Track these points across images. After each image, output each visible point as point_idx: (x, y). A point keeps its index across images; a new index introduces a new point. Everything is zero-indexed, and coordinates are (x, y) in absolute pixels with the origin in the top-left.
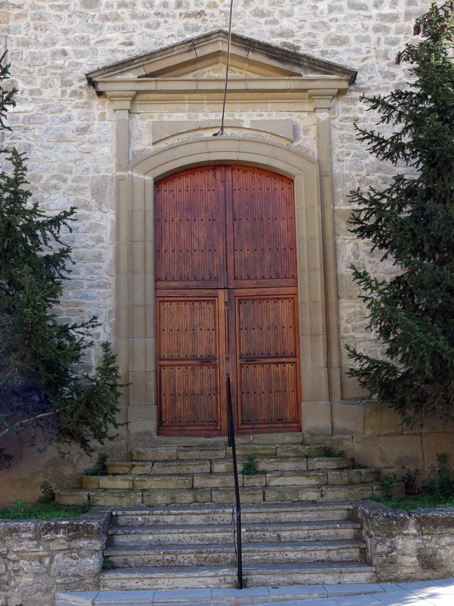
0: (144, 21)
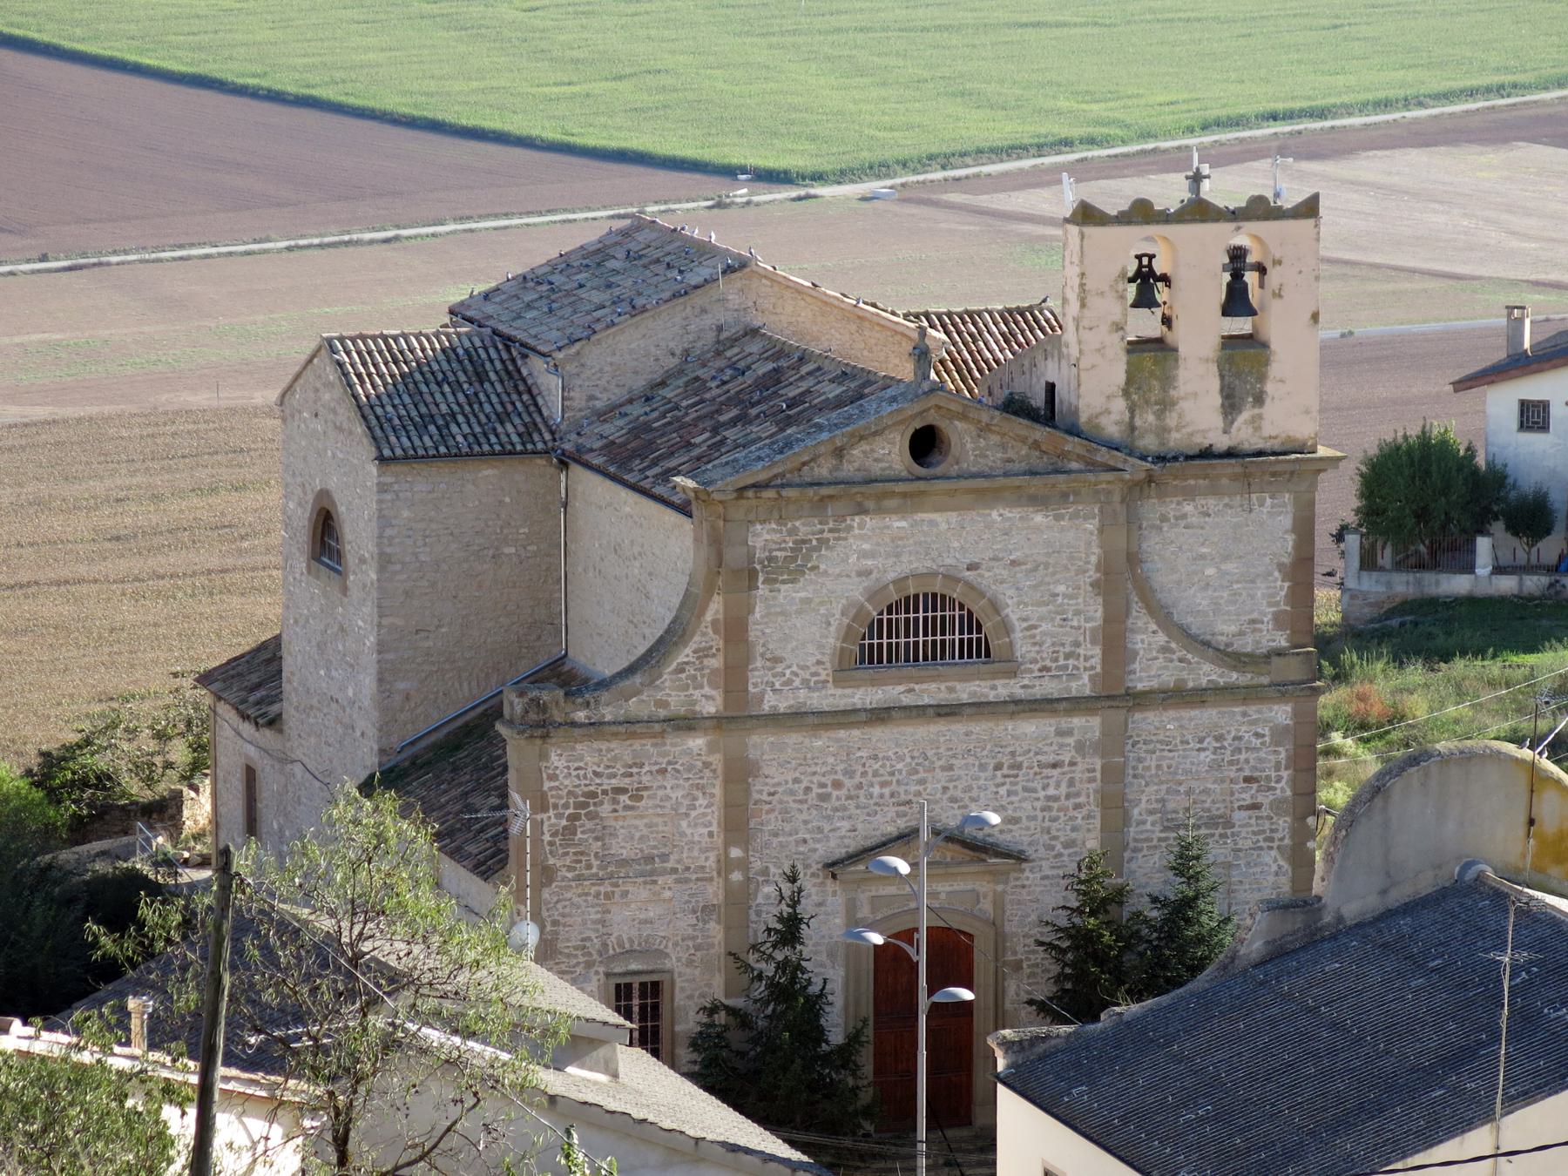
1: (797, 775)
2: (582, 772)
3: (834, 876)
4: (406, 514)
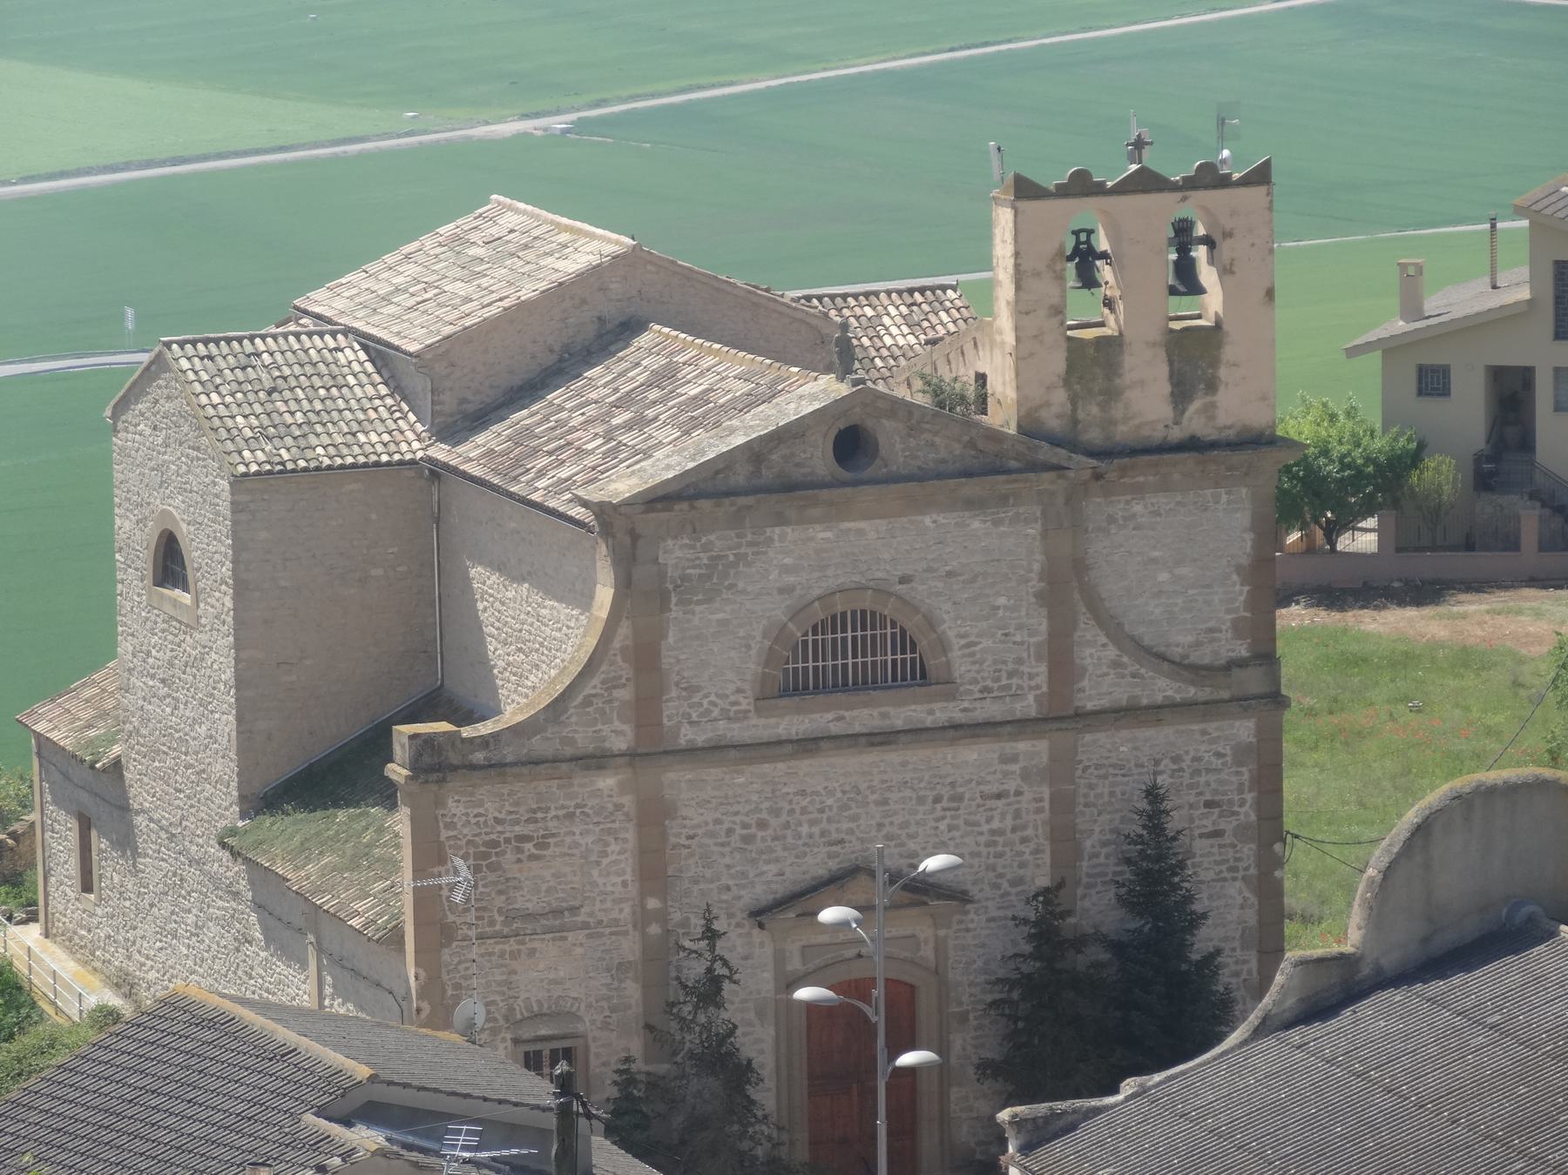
0: (794, 852)
1: (718, 815)
2: (482, 819)
3: (761, 926)
4: (263, 535)
